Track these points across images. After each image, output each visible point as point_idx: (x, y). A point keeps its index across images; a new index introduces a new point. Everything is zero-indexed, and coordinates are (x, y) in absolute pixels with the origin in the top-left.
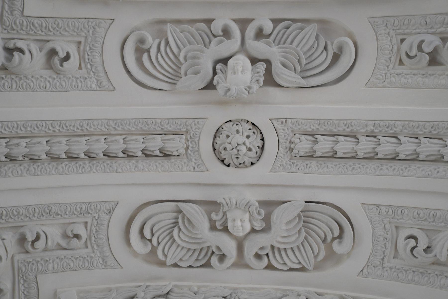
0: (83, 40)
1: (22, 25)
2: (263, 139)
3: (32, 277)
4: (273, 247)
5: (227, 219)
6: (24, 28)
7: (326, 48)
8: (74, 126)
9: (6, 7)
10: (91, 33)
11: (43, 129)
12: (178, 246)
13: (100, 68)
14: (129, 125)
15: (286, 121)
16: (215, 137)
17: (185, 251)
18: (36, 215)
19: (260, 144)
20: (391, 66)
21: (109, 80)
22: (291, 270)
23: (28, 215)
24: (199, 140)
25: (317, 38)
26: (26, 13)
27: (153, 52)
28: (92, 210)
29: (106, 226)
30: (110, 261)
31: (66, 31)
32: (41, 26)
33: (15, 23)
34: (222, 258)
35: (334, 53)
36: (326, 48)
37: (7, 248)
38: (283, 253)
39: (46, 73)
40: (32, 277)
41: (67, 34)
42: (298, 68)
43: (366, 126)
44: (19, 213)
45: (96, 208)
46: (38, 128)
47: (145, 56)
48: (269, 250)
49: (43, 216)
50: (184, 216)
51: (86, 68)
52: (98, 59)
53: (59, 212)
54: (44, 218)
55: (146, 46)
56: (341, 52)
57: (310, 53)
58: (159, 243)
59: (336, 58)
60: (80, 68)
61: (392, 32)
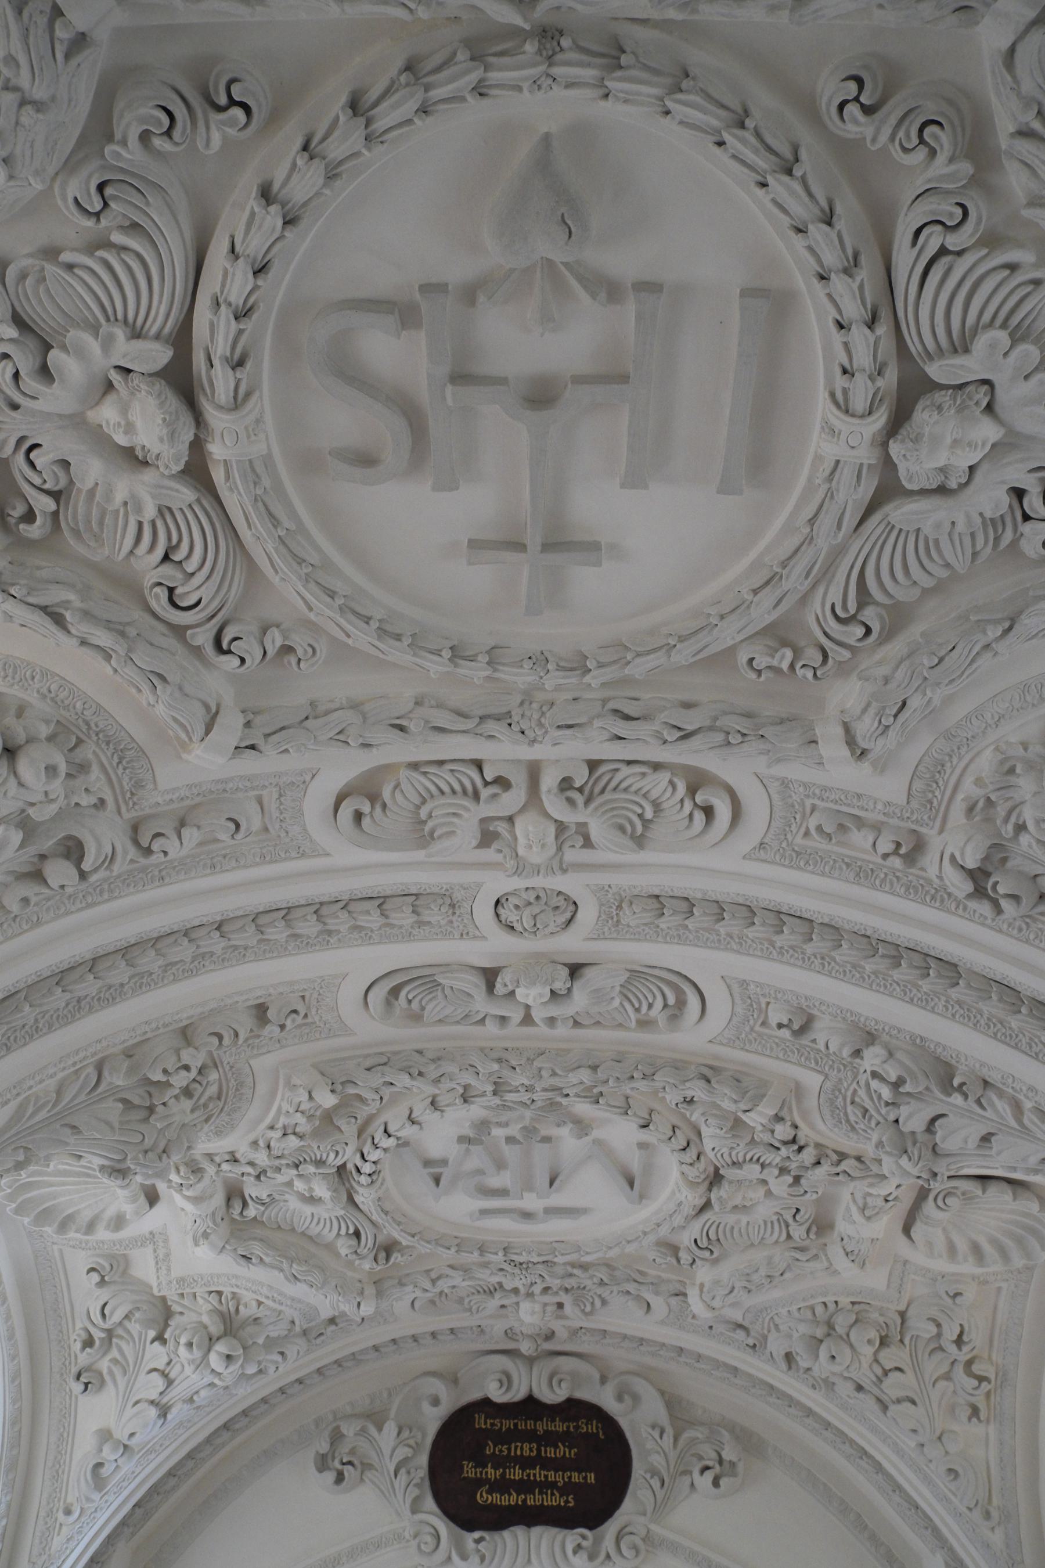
0: (757, 1028)
1: (831, 1067)
2: (497, 915)
3: (915, 804)
4: (476, 796)
5: (557, 838)
6: (831, 1063)
7: (410, 1002)
8: (792, 956)
9: (845, 1085)
10: (743, 1036)
11: (837, 968)
12: (645, 796)
13: (738, 1000)
14: (707, 939)
15: (462, 935)
16: (573, 917)
17: (633, 788)
18: (882, 876)
19: (501, 911)
20: (315, 995)
21: (729, 987)
22: (441, 763)
23: (895, 880)
24: (599, 917)
25: (423, 1009)
26: (822, 1078)
27: (659, 1003)
28: (791, 855)
29: (772, 831)
30: (774, 787)
31: (777, 1044)
32: (806, 1059)
33: (839, 1071)
34: (566, 784)
35: (397, 999)
36: (410, 1002)
37: (938, 859)
38: (457, 787)
39: (815, 1012)
40: (915, 804)
41: (777, 1040)
42: (448, 991)
43: (339, 940)
44: (908, 889)
45: (783, 856)
46: (845, 971)
47: (671, 1001)
48: (485, 793)
49: (872, 870)
50: (632, 837)
51: (759, 1004)
52: (740, 1009)
53: (844, 867)
54: (871, 866)
55: (668, 1012)
56: (387, 999)
57: (430, 996)
58: (682, 801)
59: (395, 992)
60: (768, 1003)
61: (322, 1026)
